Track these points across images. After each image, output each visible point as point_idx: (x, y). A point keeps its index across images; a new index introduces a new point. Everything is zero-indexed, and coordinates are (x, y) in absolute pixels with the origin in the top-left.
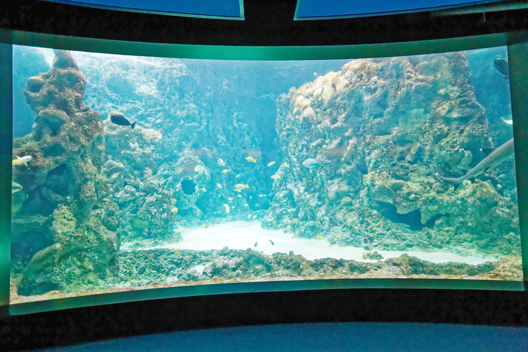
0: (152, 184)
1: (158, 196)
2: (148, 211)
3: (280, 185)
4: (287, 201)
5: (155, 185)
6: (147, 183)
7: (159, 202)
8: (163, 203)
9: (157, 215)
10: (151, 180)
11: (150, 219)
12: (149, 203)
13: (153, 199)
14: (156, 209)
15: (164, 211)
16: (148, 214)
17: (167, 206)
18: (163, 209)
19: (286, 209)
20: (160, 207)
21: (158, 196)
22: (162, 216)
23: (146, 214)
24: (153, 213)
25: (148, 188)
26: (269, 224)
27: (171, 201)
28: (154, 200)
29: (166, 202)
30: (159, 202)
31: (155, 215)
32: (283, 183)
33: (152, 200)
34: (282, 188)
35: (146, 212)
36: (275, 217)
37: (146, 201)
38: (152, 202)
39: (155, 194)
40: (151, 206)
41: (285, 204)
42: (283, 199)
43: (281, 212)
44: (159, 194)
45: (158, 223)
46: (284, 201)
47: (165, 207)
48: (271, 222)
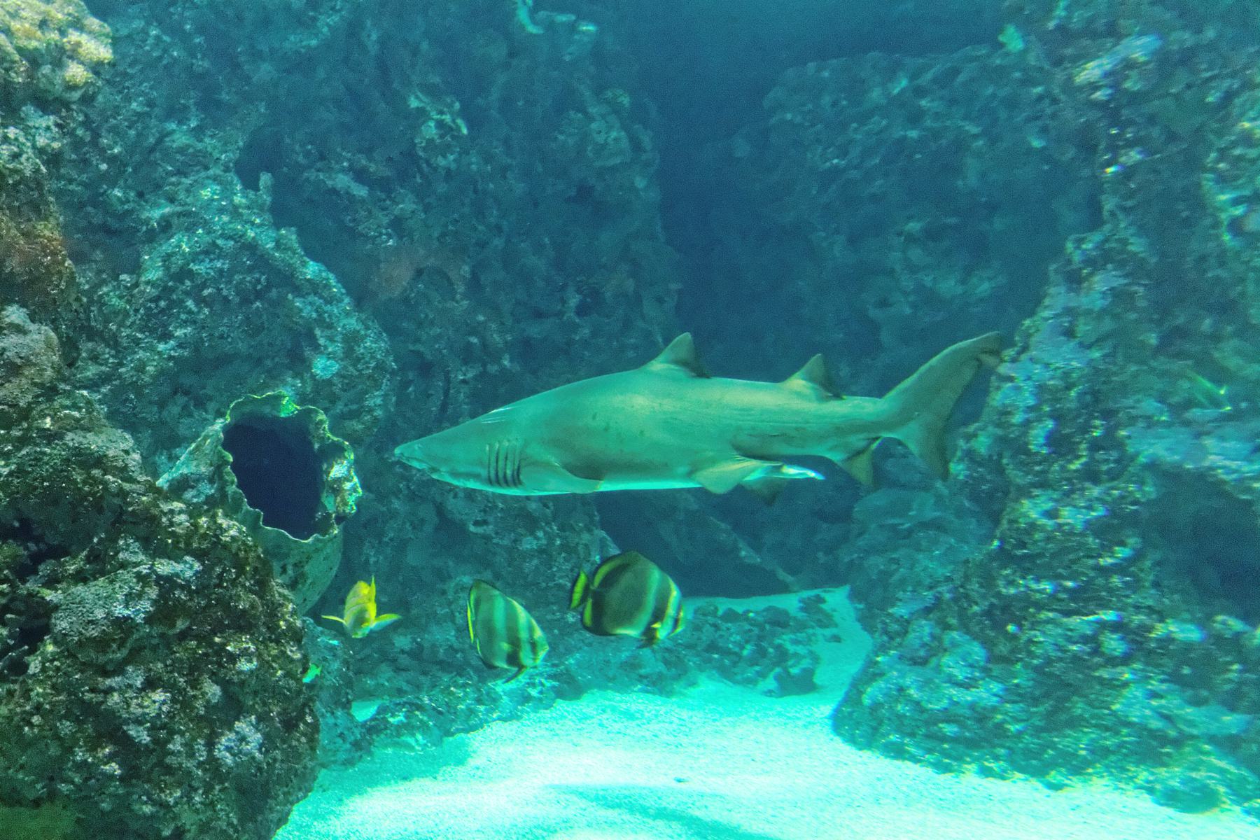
0: (99, 461)
1: (165, 567)
2: (85, 712)
3: (1060, 445)
4: (1138, 556)
5: (123, 473)
6: (37, 459)
7: (181, 625)
8: (219, 628)
9: (176, 745)
10: (78, 426)
11: (117, 788)
12: (102, 643)
13: (130, 599)
14: (159, 696)
15: (232, 707)
16: (93, 747)
17: (260, 656)
18: (225, 684)
19: (1138, 619)
20: (194, 671)
21: (165, 567)
22: (221, 752)
23: (70, 750)
24: (142, 736)
25: (52, 498)
26: (949, 729)
27: (273, 612)
28: (145, 606)
29: (242, 623)
30: (181, 625)
31: (160, 745)
32: (1086, 428)
33: (120, 611)
34: (1075, 466)
35: (66, 727)
36: (1022, 678)
37: (62, 624)
38: (123, 624)
39: (131, 551)
40: (119, 670)
41: (1116, 580)
42: (1092, 541)
43: (1085, 639)
44: (173, 554)
45: (188, 819)
46: (1106, 561)
47: (245, 666)
48: (981, 715)
